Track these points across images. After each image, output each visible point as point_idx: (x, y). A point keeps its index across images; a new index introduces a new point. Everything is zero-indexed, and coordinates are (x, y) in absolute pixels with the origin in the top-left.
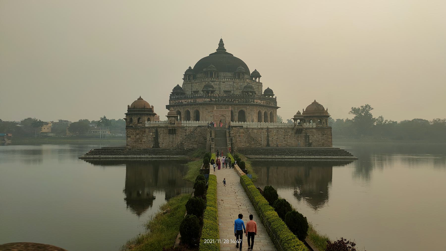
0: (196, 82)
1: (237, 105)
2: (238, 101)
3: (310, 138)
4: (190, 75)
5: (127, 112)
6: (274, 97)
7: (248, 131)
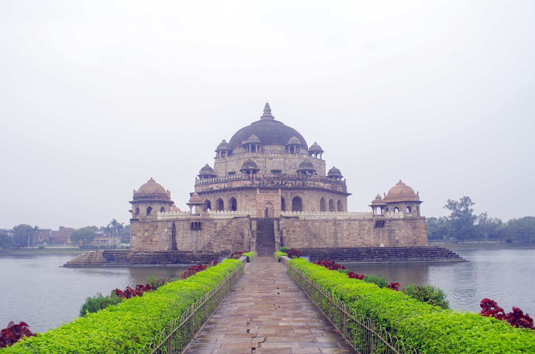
0: (232, 159)
1: (289, 189)
2: (292, 183)
3: (396, 234)
4: (224, 151)
5: (132, 200)
6: (343, 179)
7: (307, 224)
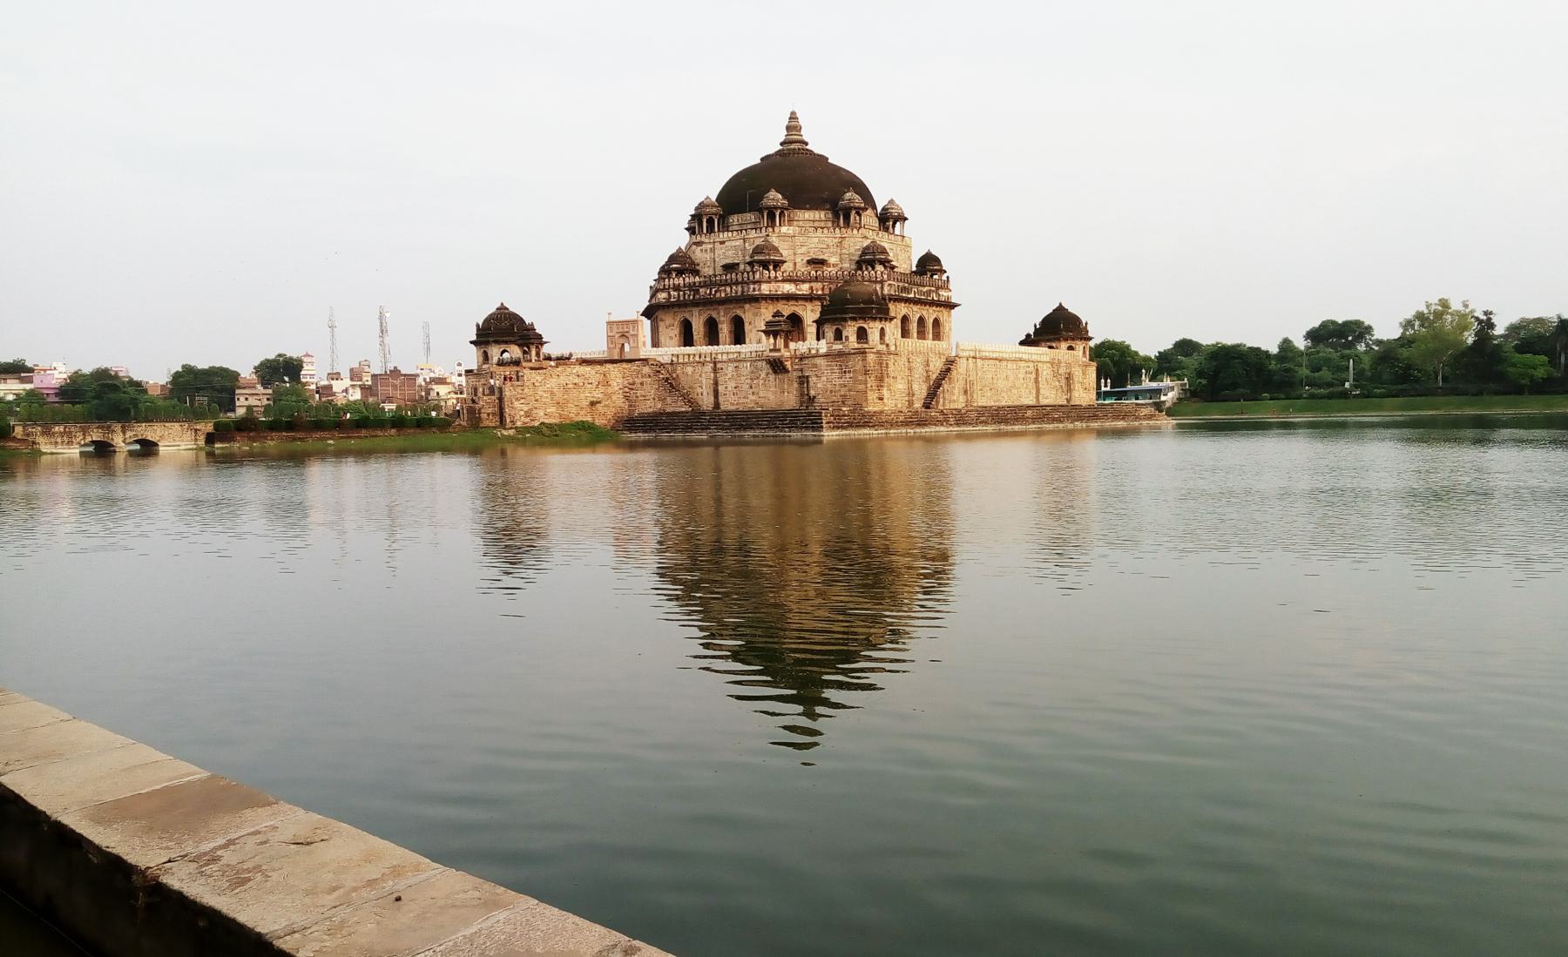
7: (675, 371)
